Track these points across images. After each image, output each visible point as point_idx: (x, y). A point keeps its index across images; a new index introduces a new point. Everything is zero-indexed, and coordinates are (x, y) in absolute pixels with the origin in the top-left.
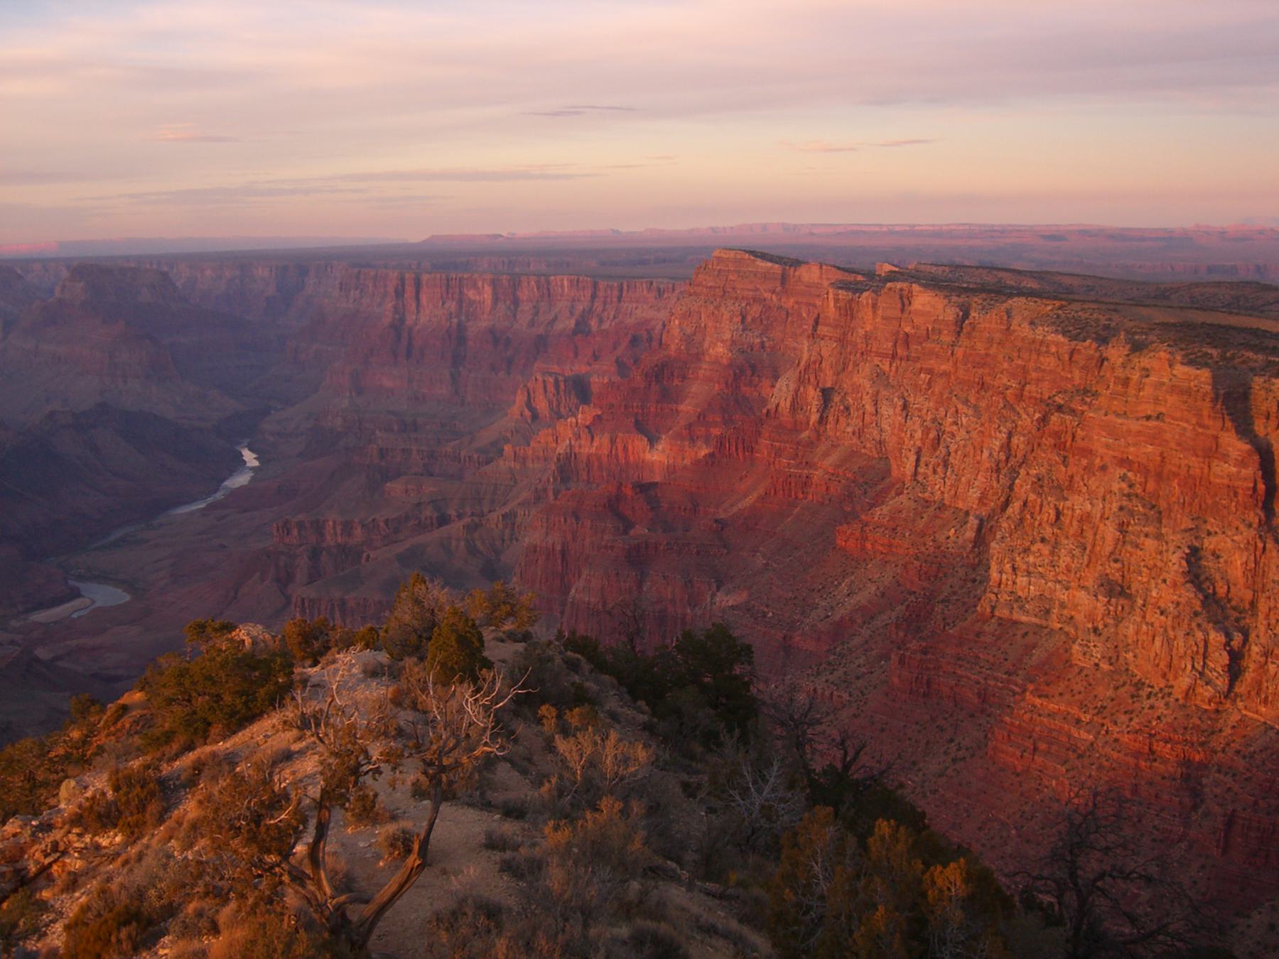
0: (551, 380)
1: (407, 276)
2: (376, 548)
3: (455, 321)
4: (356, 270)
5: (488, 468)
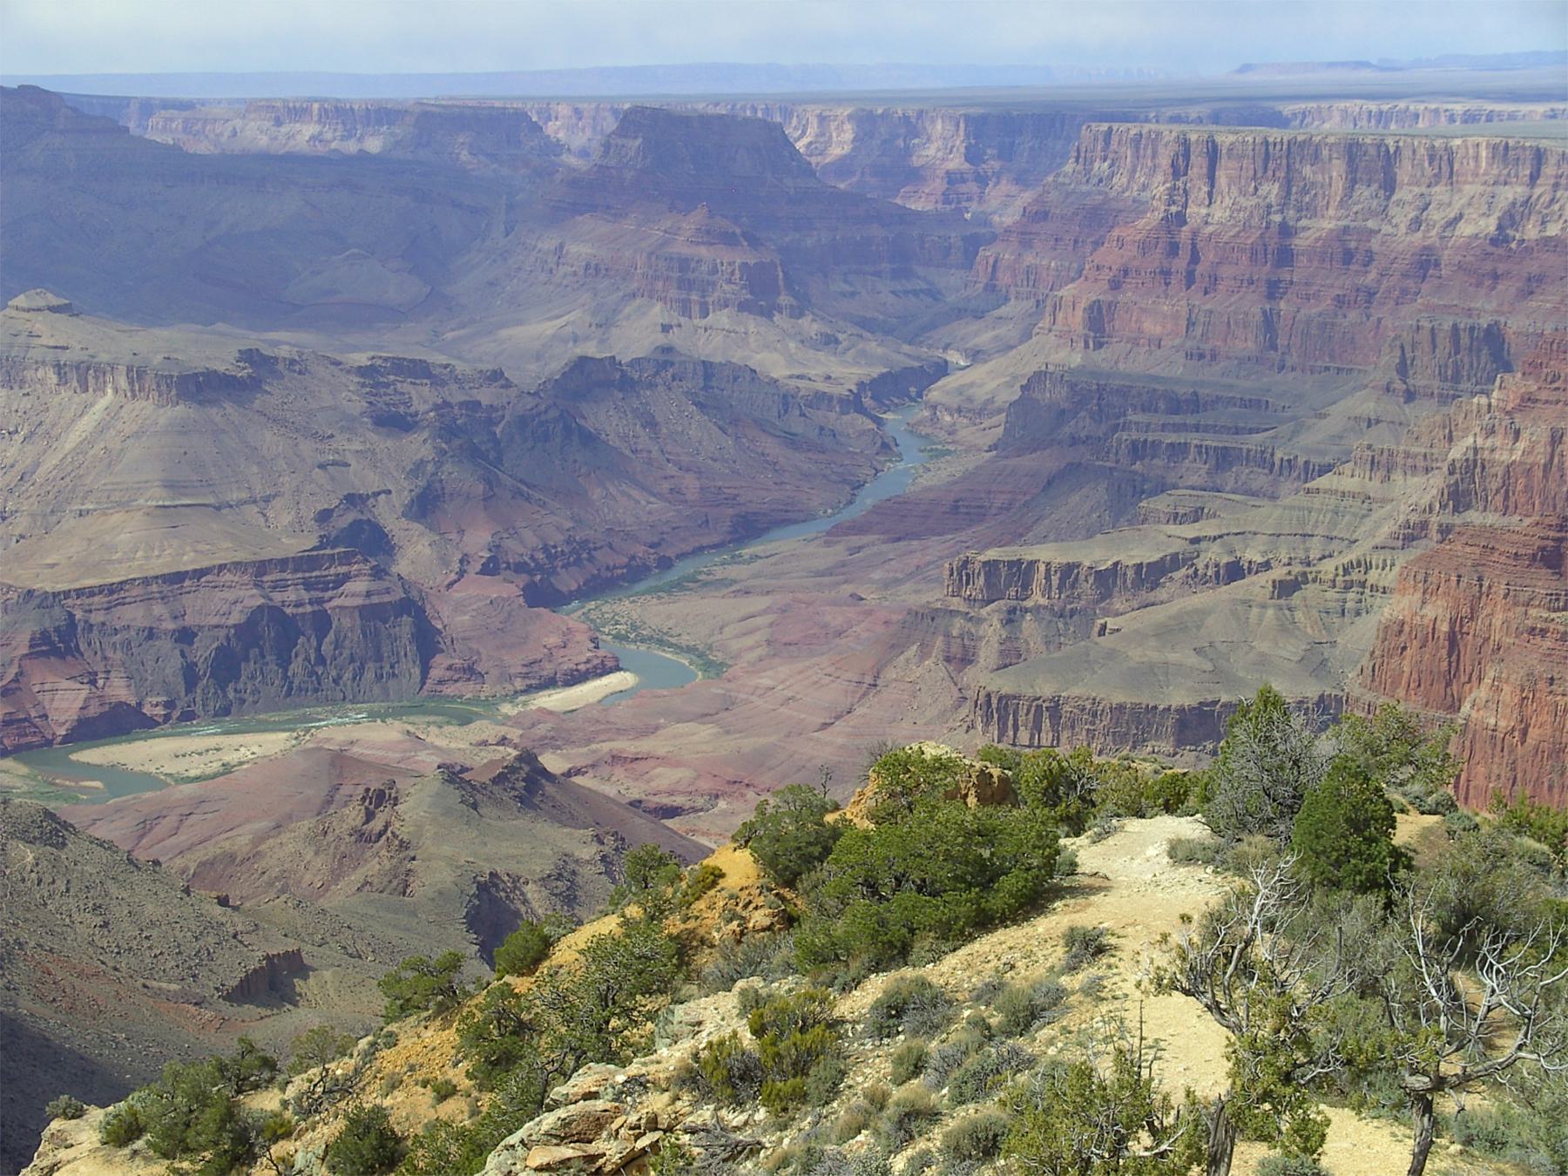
0: (1447, 326)
1: (1193, 137)
2: (1117, 614)
3: (1277, 218)
4: (1104, 127)
5: (1323, 482)
